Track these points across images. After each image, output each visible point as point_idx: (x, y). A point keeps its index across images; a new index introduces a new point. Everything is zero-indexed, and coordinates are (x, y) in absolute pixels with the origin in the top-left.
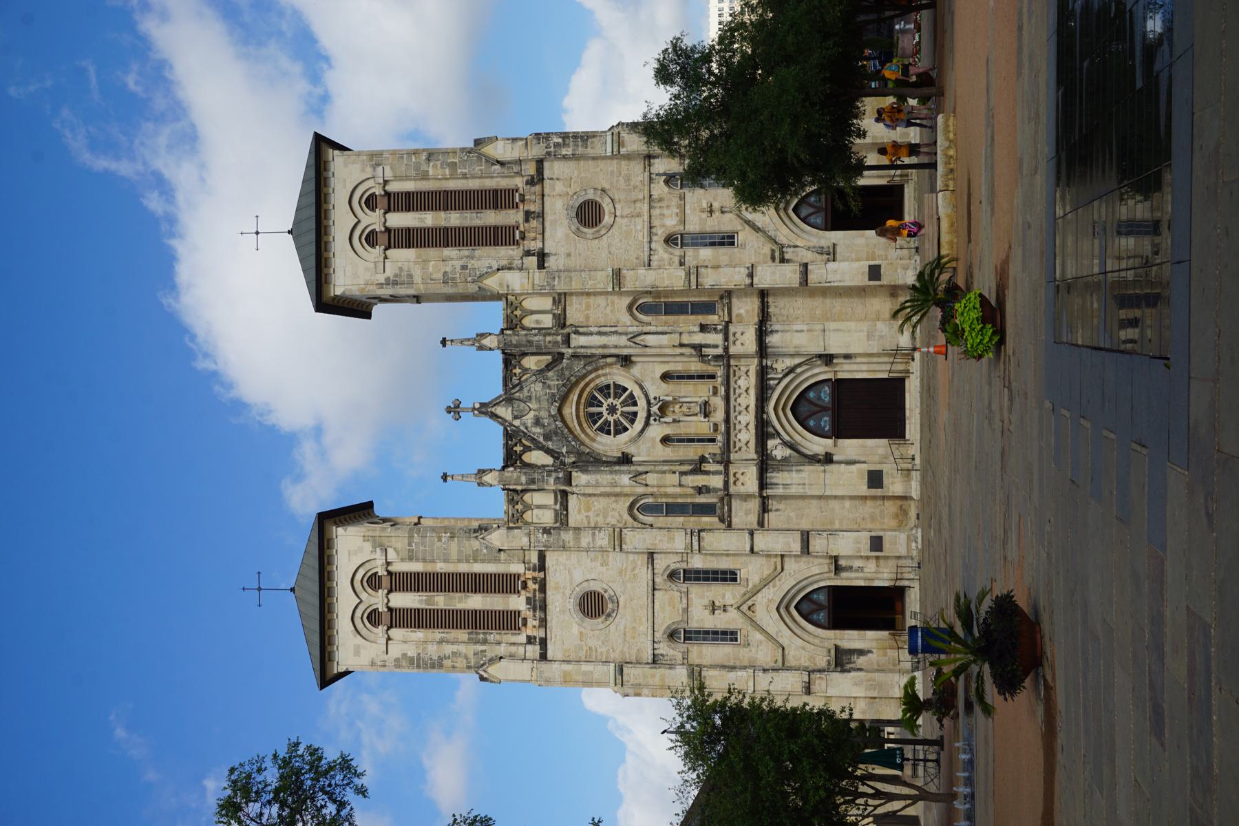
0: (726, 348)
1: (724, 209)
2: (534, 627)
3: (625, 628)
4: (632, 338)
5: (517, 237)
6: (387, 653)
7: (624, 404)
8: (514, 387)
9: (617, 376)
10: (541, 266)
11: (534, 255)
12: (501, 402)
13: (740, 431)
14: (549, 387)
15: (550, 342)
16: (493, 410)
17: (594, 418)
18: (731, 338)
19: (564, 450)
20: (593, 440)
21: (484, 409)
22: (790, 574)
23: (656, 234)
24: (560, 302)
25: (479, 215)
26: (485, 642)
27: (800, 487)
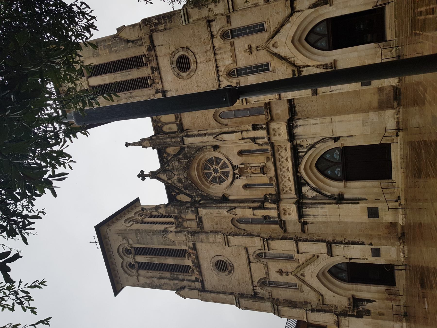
1: (259, 48)
2: (197, 274)
4: (215, 137)
6: (138, 281)
8: (165, 165)
9: (216, 154)
12: (161, 171)
15: (174, 142)
16: (158, 175)
17: (208, 175)
18: (272, 132)
19: (195, 194)
20: (209, 188)
21: (154, 175)
22: (322, 259)
23: (221, 71)
24: (178, 117)
25: (129, 73)
26: (177, 279)
27: (324, 216)
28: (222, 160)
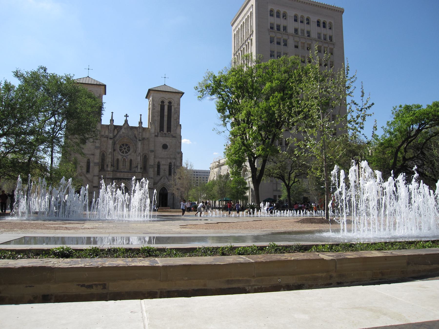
0: (137, 172)
5: (161, 132)
9: (131, 150)
10: (155, 136)
21: (126, 121)
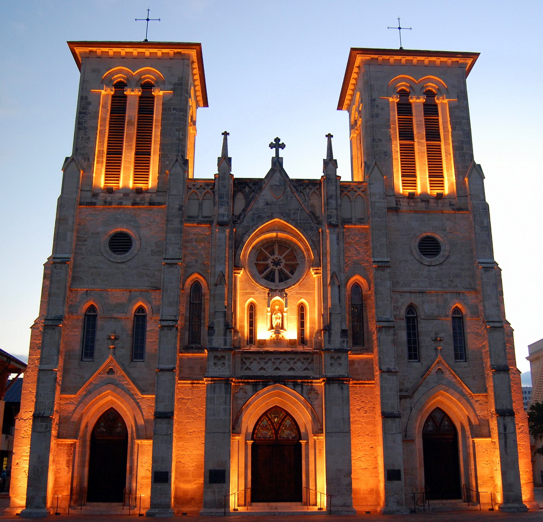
3: (100, 268)
7: (281, 272)
11: (397, 204)
13: (259, 363)
14: (294, 213)
18: (336, 356)
28: (293, 275)
